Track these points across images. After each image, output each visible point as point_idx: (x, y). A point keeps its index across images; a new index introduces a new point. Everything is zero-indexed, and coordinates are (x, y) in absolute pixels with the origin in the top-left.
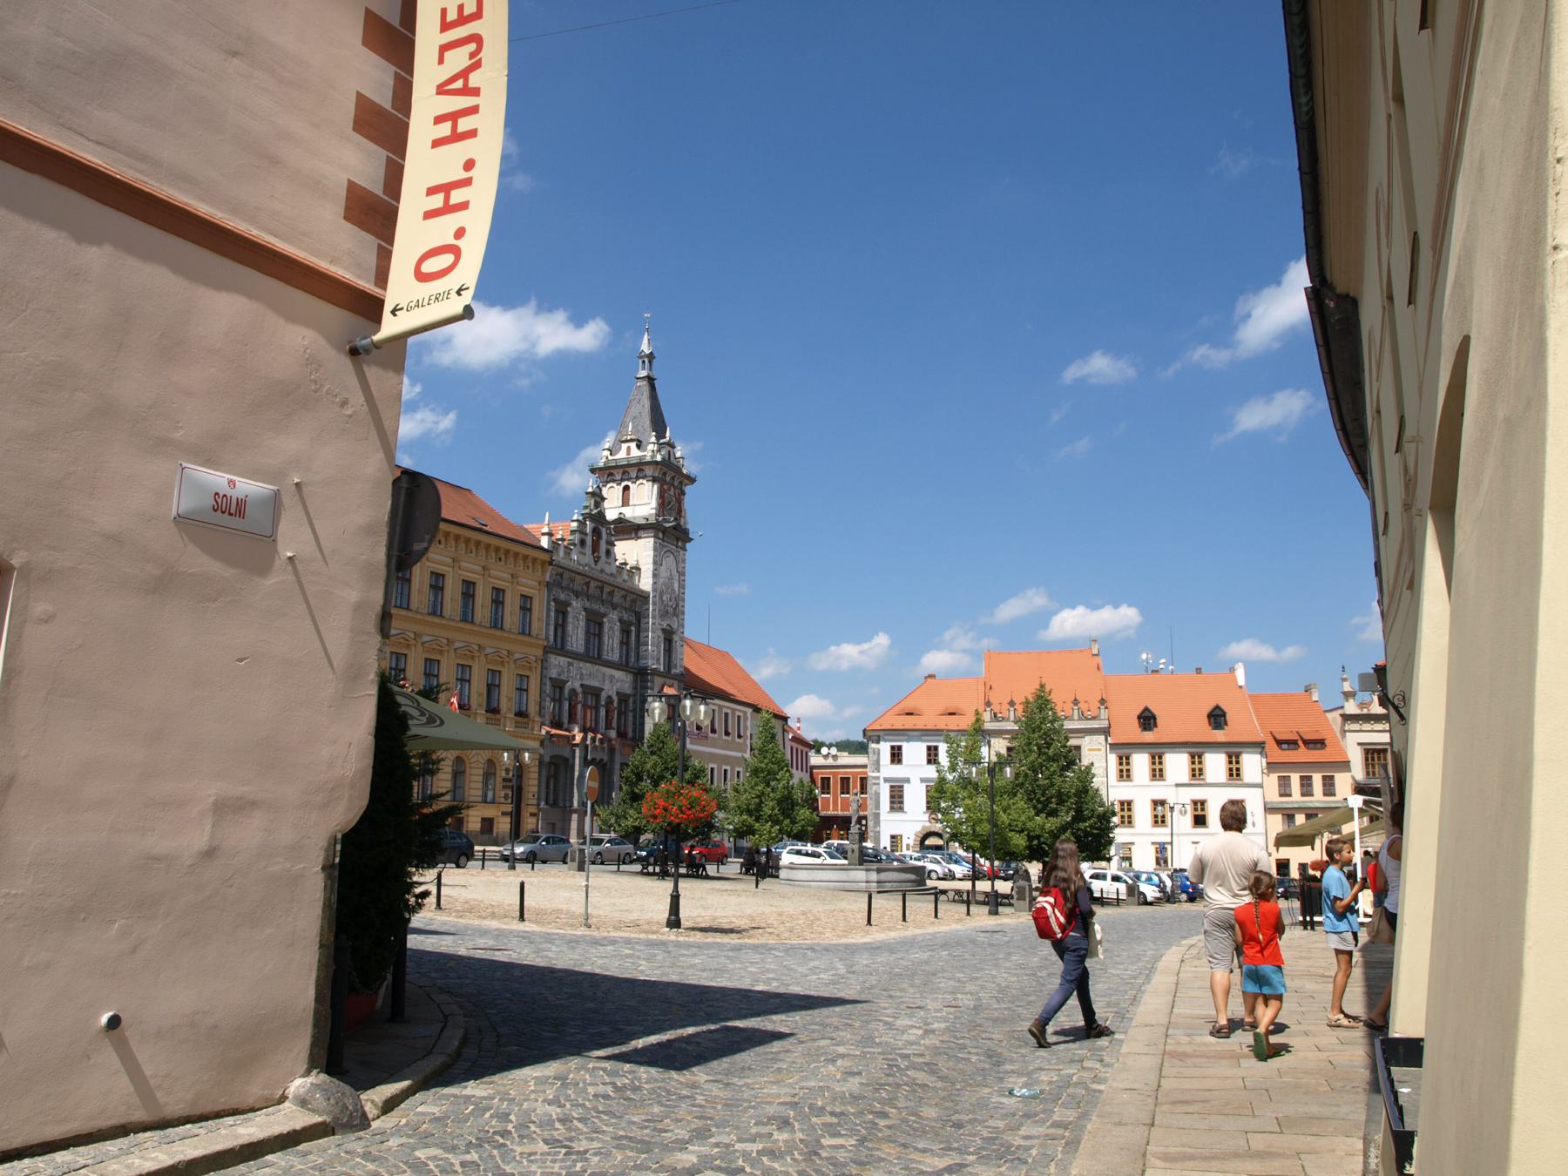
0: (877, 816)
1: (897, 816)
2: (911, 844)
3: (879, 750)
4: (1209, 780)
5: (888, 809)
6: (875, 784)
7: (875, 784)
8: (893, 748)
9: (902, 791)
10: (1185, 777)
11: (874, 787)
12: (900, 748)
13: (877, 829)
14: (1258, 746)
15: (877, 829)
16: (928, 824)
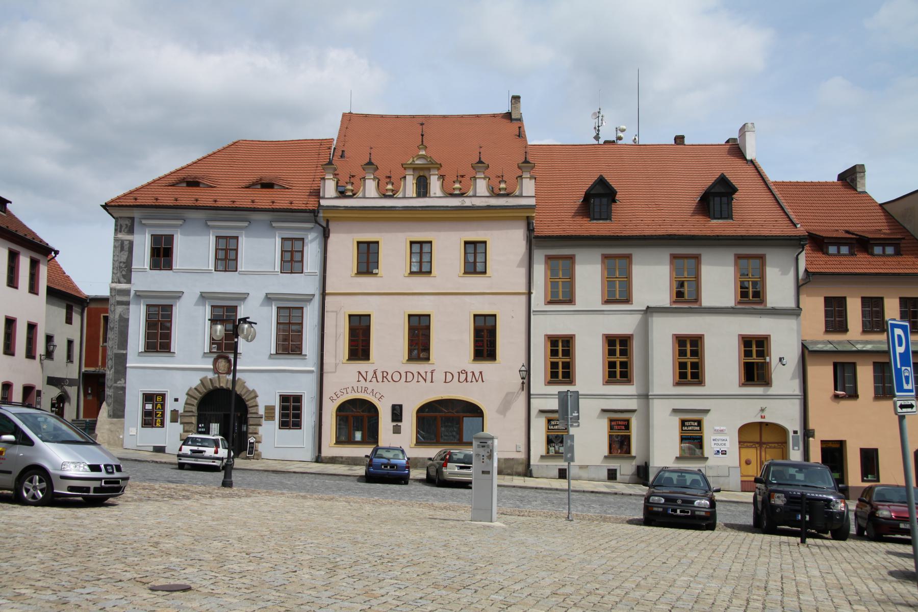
0: (122, 360)
1: (158, 361)
2: (180, 407)
3: (131, 243)
4: (706, 301)
5: (141, 348)
6: (120, 303)
7: (120, 303)
8: (156, 238)
9: (170, 316)
10: (664, 298)
11: (119, 309)
12: (170, 239)
13: (120, 384)
14: (793, 242)
15: (120, 384)
16: (210, 375)
